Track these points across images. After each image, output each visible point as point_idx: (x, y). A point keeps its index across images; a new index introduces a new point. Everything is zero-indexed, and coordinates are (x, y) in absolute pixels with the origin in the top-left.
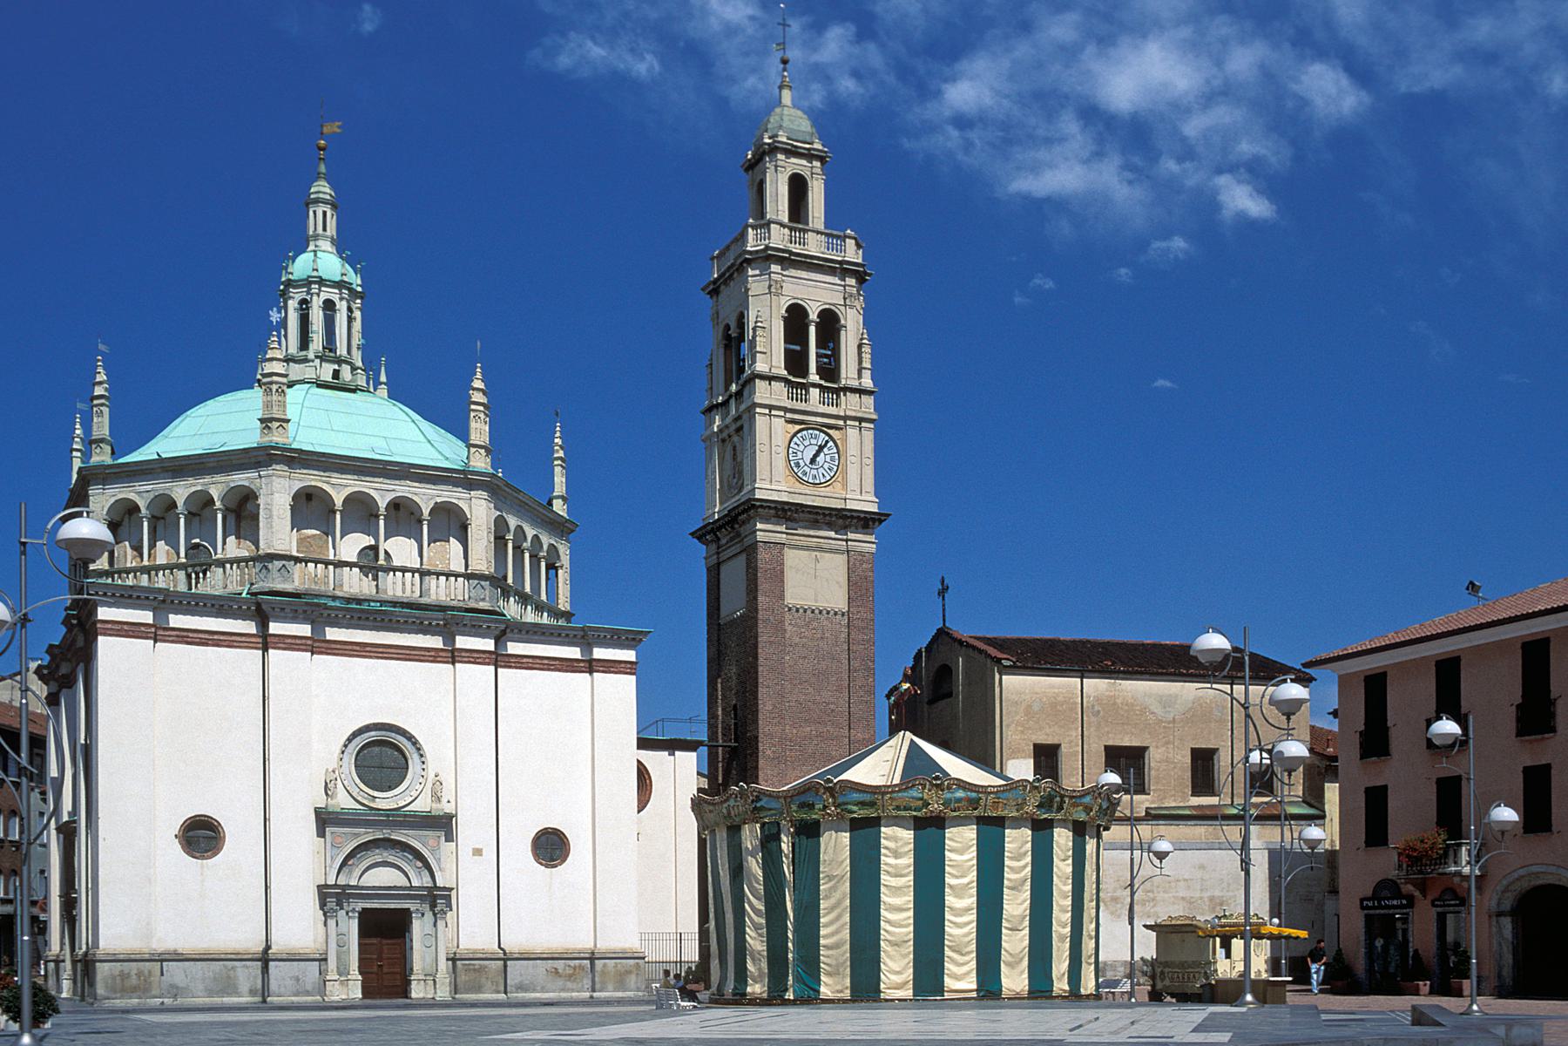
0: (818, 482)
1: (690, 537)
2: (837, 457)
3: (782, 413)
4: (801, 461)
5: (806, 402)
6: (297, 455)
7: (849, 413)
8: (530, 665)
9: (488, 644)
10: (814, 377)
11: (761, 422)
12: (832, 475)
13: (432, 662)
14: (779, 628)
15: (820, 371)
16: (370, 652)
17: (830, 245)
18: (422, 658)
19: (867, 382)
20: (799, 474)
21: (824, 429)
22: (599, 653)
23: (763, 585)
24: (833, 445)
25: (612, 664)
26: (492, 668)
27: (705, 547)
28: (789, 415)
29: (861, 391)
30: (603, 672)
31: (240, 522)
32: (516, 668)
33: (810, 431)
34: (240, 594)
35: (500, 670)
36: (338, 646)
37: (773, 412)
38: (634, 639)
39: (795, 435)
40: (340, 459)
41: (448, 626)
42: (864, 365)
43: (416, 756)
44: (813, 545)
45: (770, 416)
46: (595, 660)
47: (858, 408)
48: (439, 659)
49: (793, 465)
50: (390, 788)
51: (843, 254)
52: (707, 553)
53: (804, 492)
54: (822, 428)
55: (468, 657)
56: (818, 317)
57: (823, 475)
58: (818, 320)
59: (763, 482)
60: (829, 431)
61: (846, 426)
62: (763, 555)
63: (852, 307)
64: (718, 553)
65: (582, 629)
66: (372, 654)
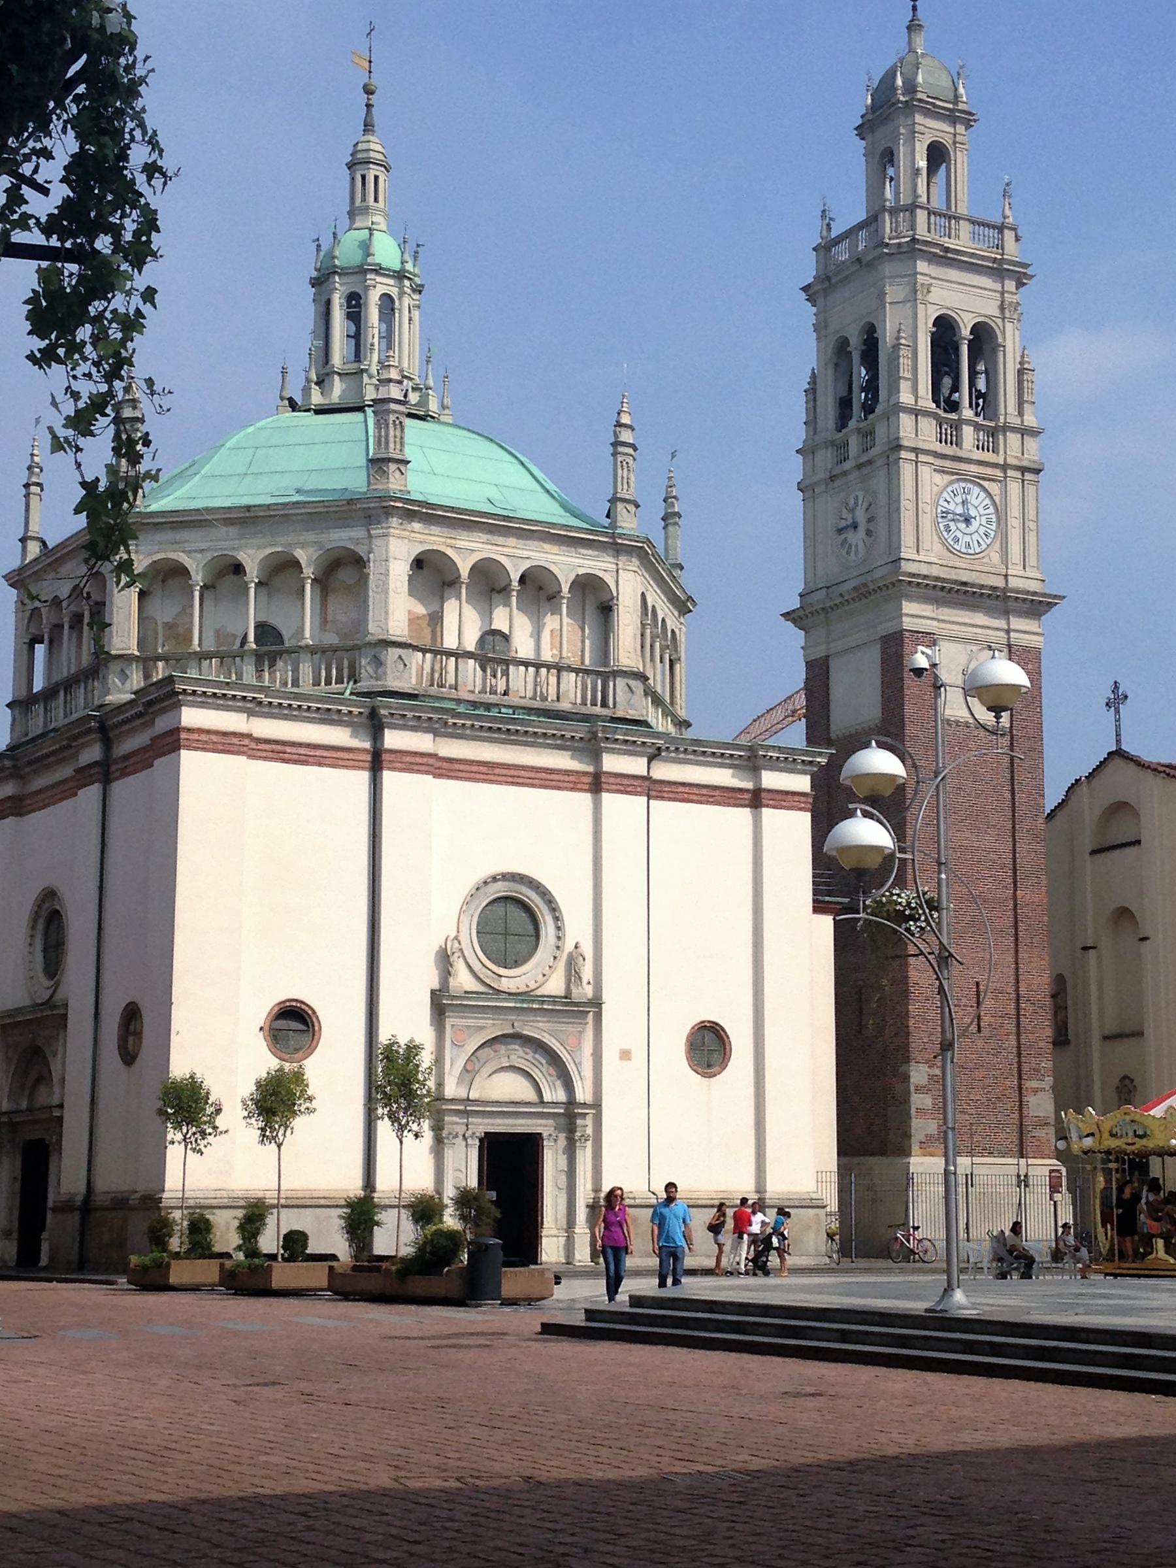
1: (782, 619)
2: (993, 516)
3: (930, 459)
5: (957, 445)
6: (400, 505)
7: (1009, 461)
9: (636, 765)
10: (968, 413)
11: (906, 471)
12: (988, 541)
13: (572, 789)
17: (976, 236)
18: (560, 784)
21: (981, 482)
25: (784, 797)
26: (646, 798)
27: (803, 632)
28: (938, 462)
30: (774, 807)
31: (327, 595)
32: (670, 799)
33: (963, 485)
34: (343, 694)
35: (651, 801)
37: (922, 458)
39: (945, 489)
43: (549, 919)
44: (970, 636)
45: (916, 463)
46: (769, 791)
47: (1020, 455)
48: (579, 786)
49: (942, 529)
50: (517, 964)
51: (1000, 251)
53: (958, 564)
54: (977, 480)
56: (971, 333)
58: (972, 337)
60: (981, 482)
61: (1006, 477)
64: (829, 643)
65: (751, 749)
66: (500, 778)
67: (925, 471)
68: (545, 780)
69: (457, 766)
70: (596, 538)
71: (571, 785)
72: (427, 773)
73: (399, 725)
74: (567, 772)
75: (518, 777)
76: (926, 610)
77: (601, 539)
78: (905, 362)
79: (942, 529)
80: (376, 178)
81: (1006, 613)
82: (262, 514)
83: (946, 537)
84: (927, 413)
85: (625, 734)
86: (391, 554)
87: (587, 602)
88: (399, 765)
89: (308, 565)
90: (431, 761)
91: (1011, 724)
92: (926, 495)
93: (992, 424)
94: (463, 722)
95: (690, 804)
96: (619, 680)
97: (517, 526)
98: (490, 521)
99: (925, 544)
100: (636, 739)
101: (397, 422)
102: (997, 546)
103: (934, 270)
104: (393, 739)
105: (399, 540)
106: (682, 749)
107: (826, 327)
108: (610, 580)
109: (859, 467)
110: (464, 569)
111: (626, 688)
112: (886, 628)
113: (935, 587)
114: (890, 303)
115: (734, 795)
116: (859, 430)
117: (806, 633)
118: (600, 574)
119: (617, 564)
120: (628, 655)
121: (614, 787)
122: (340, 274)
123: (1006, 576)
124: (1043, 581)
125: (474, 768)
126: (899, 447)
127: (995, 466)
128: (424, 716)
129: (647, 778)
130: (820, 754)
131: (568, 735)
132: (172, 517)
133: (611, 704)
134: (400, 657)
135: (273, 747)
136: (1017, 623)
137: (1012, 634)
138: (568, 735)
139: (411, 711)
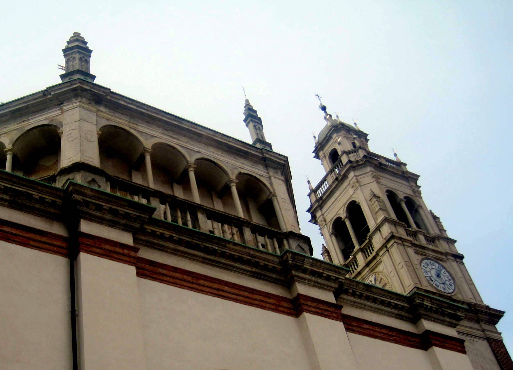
0: (447, 292)
2: (451, 279)
4: (433, 279)
6: (88, 88)
12: (453, 288)
16: (204, 286)
18: (264, 304)
33: (429, 261)
36: (165, 272)
40: (137, 106)
45: (404, 245)
48: (281, 309)
57: (449, 288)
58: (406, 200)
67: (411, 251)
69: (161, 270)
70: (249, 151)
71: (273, 307)
73: (94, 216)
75: (223, 291)
85: (312, 265)
88: (98, 250)
94: (161, 231)
98: (164, 119)
107: (325, 221)
109: (367, 265)
116: (362, 250)
118: (258, 177)
119: (268, 173)
121: (313, 310)
125: (178, 275)
139: (107, 202)
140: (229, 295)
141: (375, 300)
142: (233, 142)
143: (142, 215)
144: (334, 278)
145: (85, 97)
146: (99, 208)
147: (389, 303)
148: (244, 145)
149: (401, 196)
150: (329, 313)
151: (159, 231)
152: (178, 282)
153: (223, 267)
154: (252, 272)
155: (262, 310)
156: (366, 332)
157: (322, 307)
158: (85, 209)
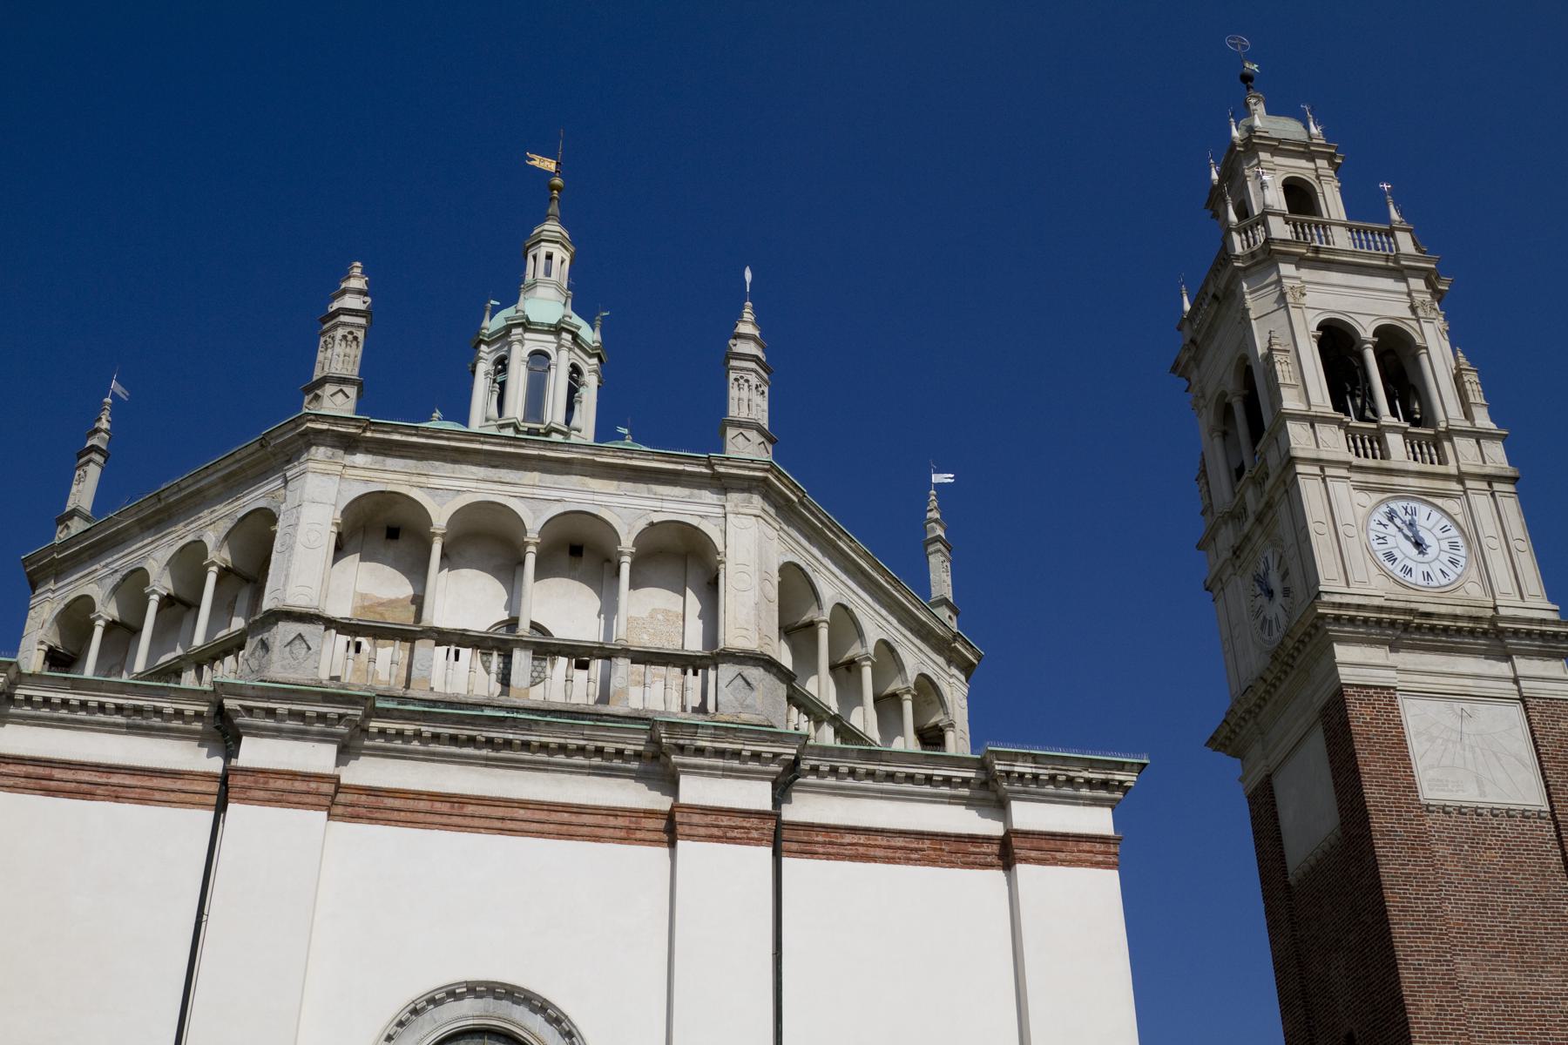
2: (1461, 542)
3: (1343, 472)
4: (1397, 553)
6: (325, 427)
8: (861, 850)
10: (1386, 418)
11: (1310, 490)
13: (622, 840)
14: (1420, 841)
15: (1394, 413)
19: (1483, 420)
20: (1396, 572)
21: (1430, 499)
22: (1028, 815)
23: (1370, 765)
24: (1449, 524)
26: (766, 852)
27: (1239, 760)
29: (1479, 436)
32: (828, 856)
33: (1404, 504)
35: (787, 862)
36: (397, 803)
37: (1329, 471)
38: (1105, 784)
41: (662, 758)
42: (1472, 400)
45: (1324, 480)
46: (1026, 834)
47: (1481, 463)
48: (639, 835)
52: (1243, 770)
54: (1424, 496)
55: (707, 826)
57: (1442, 572)
58: (1376, 340)
59: (1332, 583)
61: (1465, 492)
62: (1360, 715)
63: (1430, 321)
66: (477, 822)
67: (1340, 490)
68: (570, 824)
69: (390, 802)
70: (680, 467)
71: (622, 834)
72: (316, 806)
74: (613, 812)
76: (1379, 655)
77: (689, 468)
78: (1284, 372)
79: (1382, 558)
80: (549, 257)
81: (1507, 657)
82: (172, 500)
83: (1391, 567)
84: (1325, 420)
85: (715, 738)
86: (305, 497)
87: (690, 577)
88: (262, 794)
89: (219, 548)
90: (328, 788)
91: (1552, 807)
92: (1345, 514)
93: (1430, 432)
94: (397, 726)
95: (872, 865)
96: (722, 667)
97: (536, 452)
99: (1356, 574)
100: (740, 747)
101: (350, 337)
102: (1474, 573)
103: (1306, 274)
104: (255, 752)
105: (325, 478)
106: (844, 770)
108: (711, 529)
109: (1259, 519)
110: (440, 515)
111: (740, 681)
112: (1322, 697)
113: (1379, 622)
114: (1255, 319)
115: (962, 846)
117: (1242, 760)
119: (724, 506)
120: (744, 632)
121: (702, 831)
122: (488, 344)
123: (1495, 608)
124: (1557, 610)
125: (422, 805)
126: (1292, 461)
127: (1446, 477)
128: (311, 709)
129: (775, 815)
130: (1121, 766)
131: (610, 747)
132: (87, 539)
133: (711, 706)
134: (300, 636)
135: (31, 769)
136: (1524, 666)
137: (1523, 683)
138: (610, 747)
140: (525, 826)
141: (890, 777)
142: (642, 457)
143: (350, 712)
144: (770, 756)
145: (323, 445)
146: (271, 713)
147: (929, 780)
148: (667, 459)
149: (1366, 330)
150: (741, 833)
151: (392, 726)
152: (420, 817)
153: (529, 768)
154: (590, 767)
155: (593, 844)
156: (849, 851)
157: (725, 823)
158: (246, 720)
